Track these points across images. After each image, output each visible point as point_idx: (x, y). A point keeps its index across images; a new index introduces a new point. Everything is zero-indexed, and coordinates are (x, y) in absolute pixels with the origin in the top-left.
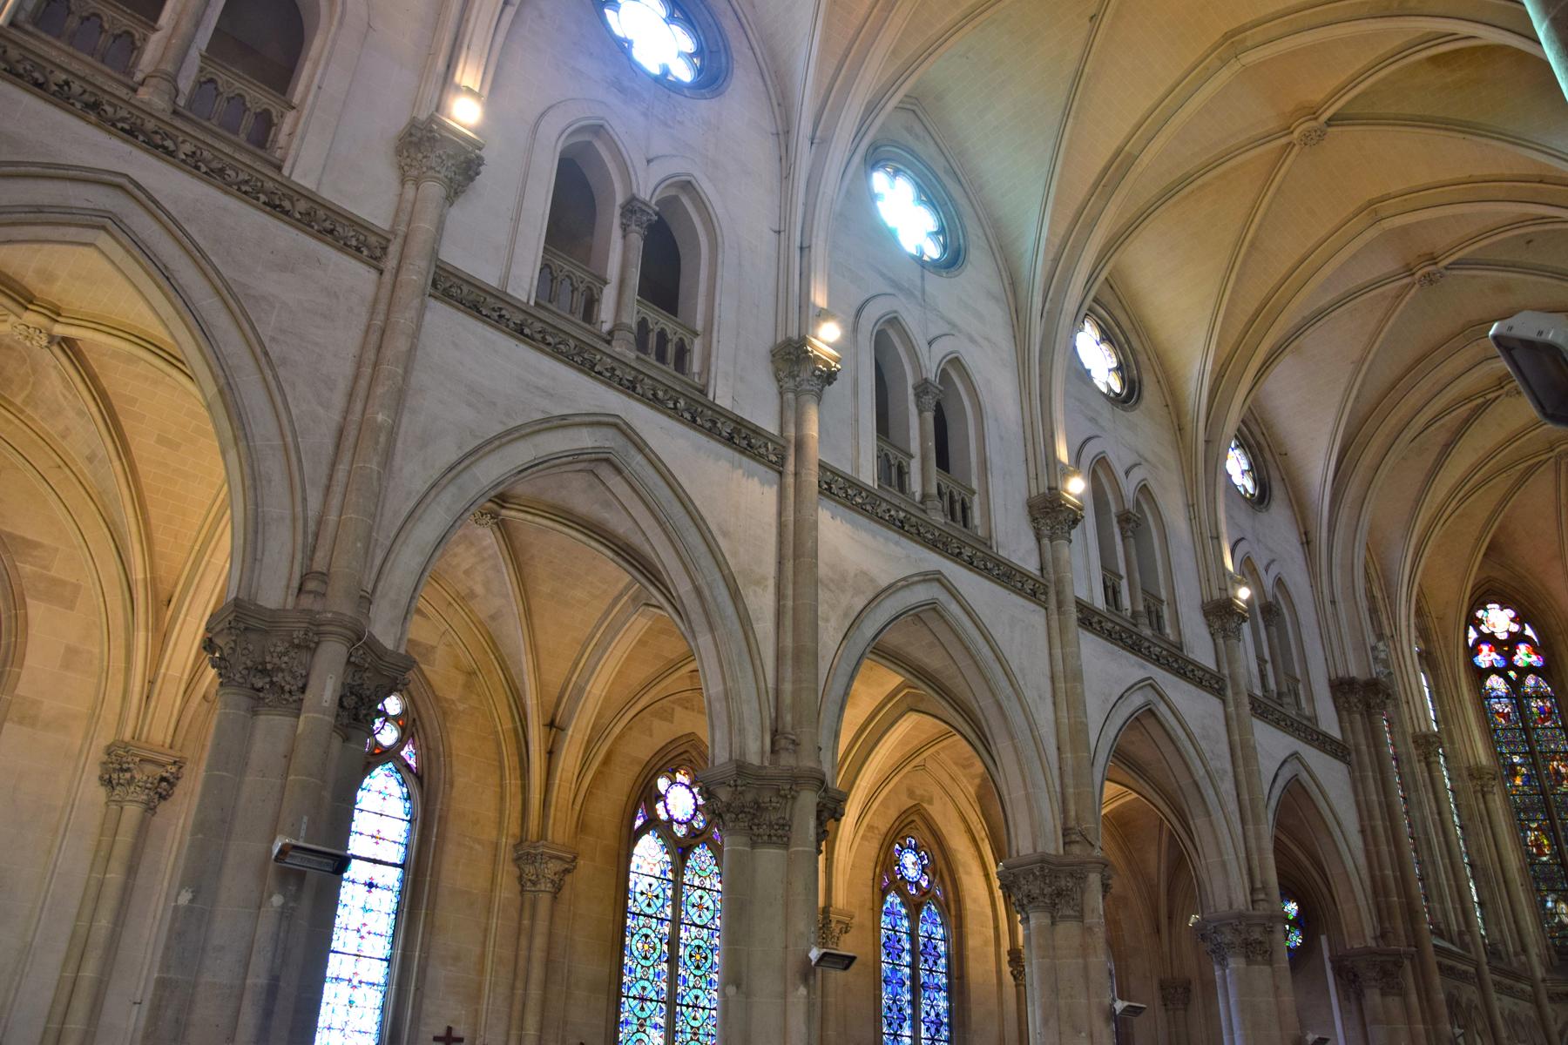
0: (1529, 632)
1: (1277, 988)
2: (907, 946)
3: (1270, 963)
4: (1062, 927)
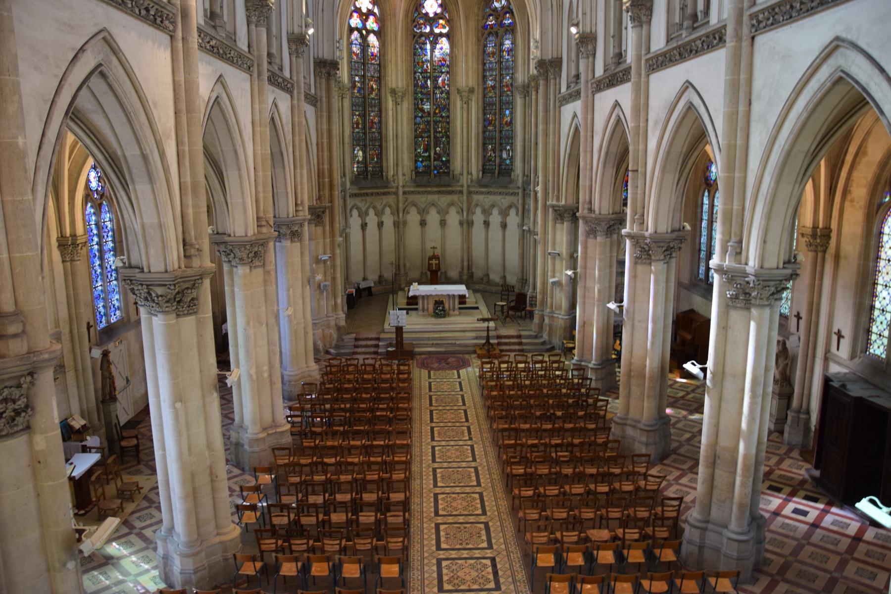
0: (376, 10)
1: (302, 254)
2: (95, 232)
4: (255, 271)
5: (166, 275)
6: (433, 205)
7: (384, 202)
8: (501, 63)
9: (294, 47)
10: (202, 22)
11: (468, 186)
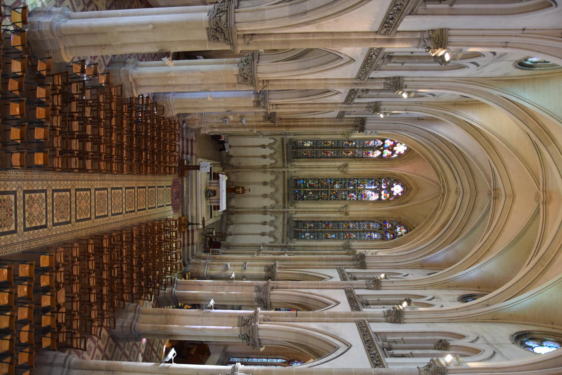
0: (395, 156)
1: (246, 107)
3: (254, 107)
4: (235, 78)
5: (233, 23)
6: (277, 190)
7: (279, 160)
8: (364, 232)
9: (372, 105)
10: (386, 50)
11: (288, 212)
